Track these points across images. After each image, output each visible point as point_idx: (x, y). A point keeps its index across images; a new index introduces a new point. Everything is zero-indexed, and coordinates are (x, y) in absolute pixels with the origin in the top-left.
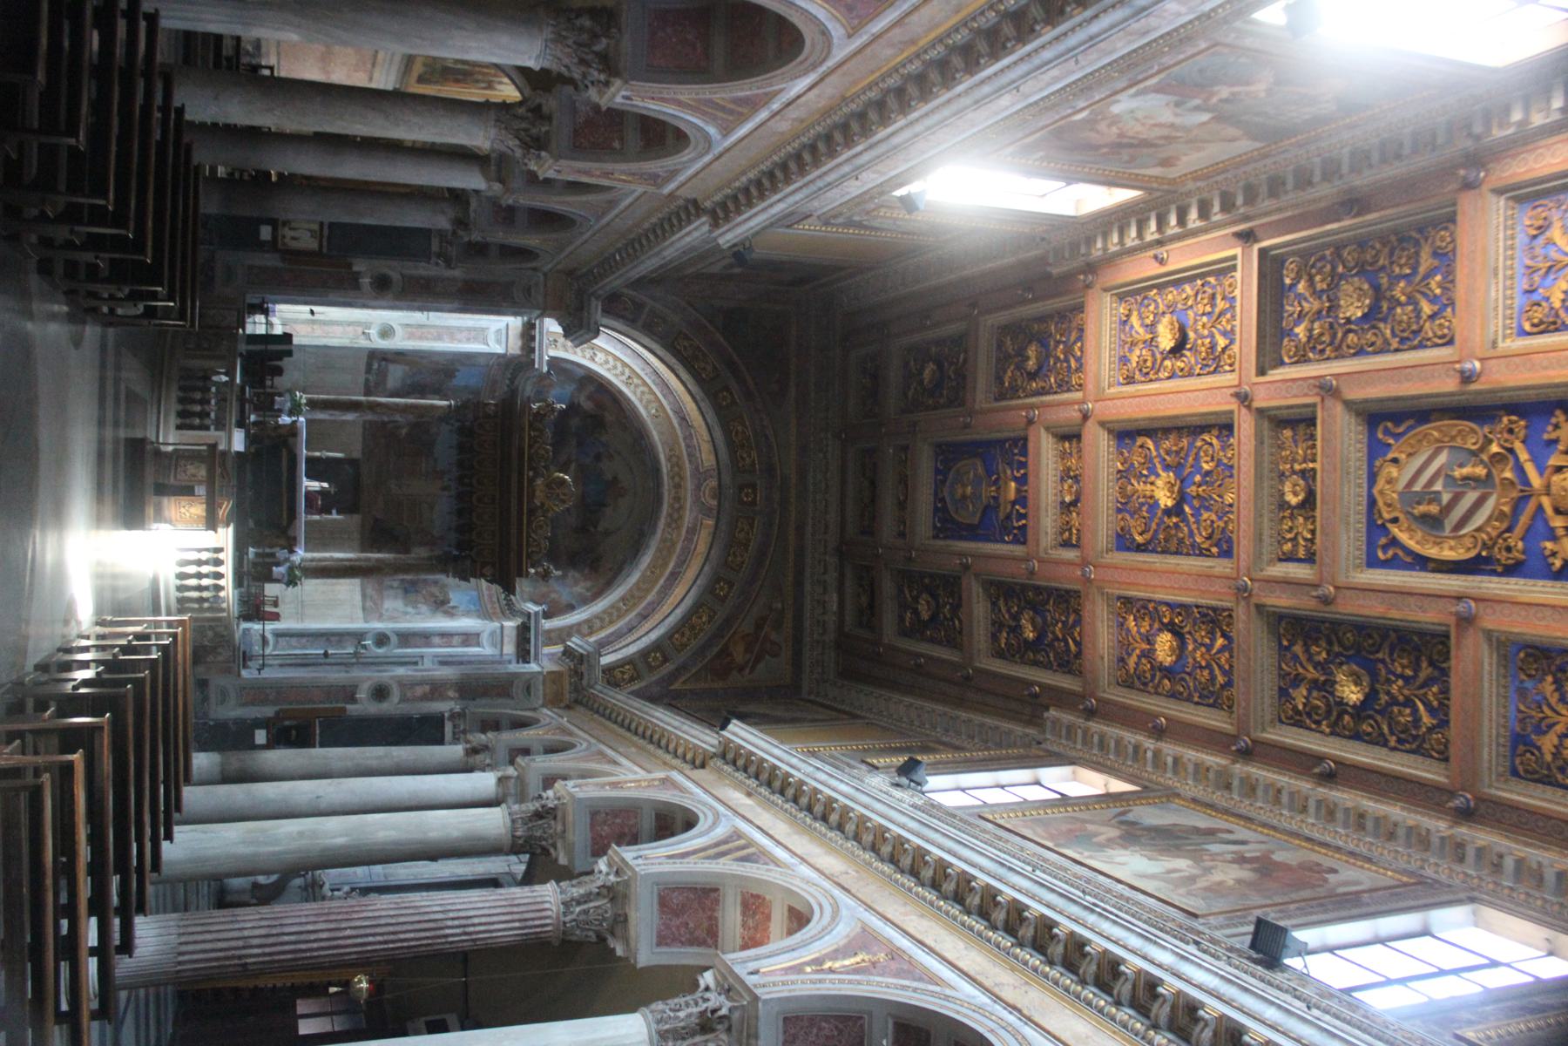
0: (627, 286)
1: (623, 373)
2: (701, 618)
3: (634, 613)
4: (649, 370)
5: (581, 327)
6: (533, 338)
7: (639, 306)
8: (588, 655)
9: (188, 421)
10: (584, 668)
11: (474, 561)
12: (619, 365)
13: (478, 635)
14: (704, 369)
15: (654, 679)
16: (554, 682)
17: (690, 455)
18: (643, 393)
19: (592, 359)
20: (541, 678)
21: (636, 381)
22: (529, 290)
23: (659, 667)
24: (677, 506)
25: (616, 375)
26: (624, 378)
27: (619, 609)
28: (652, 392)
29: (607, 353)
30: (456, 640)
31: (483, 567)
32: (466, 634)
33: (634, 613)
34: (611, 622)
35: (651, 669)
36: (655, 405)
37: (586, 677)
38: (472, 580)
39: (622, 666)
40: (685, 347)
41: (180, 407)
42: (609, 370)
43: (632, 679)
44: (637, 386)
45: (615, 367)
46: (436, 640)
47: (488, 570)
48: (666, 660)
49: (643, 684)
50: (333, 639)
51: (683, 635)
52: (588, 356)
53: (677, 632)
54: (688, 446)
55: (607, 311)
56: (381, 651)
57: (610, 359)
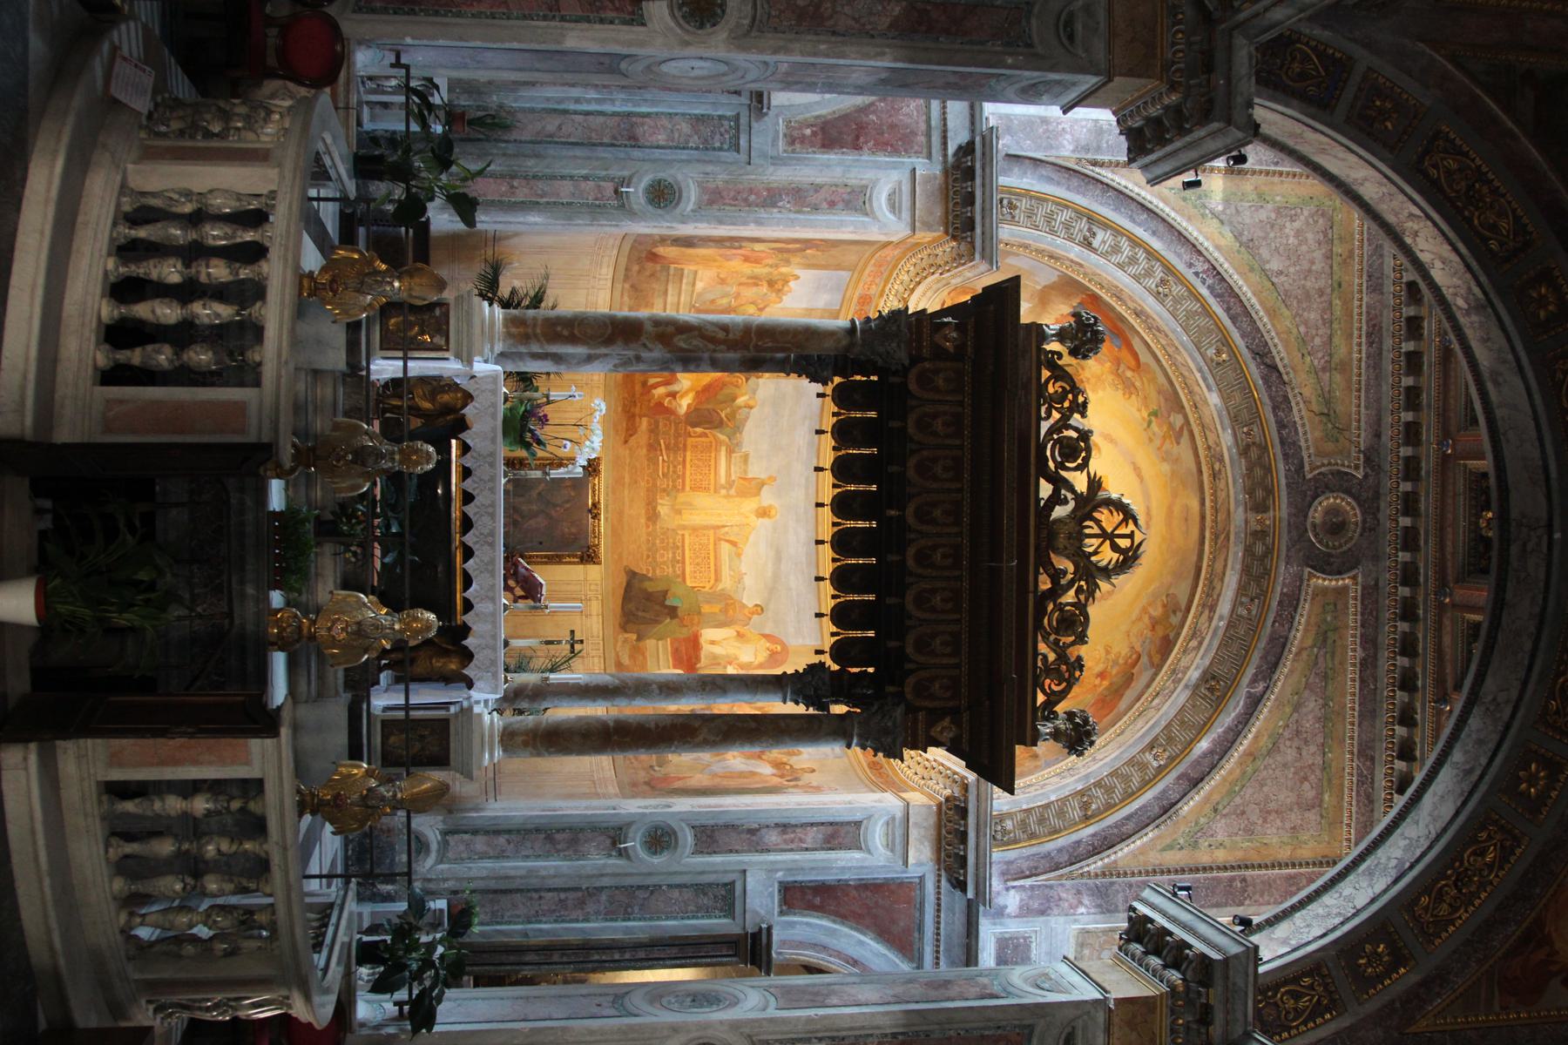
0: (1310, 19)
1: (1149, 273)
2: (1483, 853)
3: (1174, 774)
4: (1201, 266)
5: (1206, 116)
6: (970, 200)
7: (1338, 67)
8: (1227, 961)
9: (135, 357)
10: (1215, 996)
11: (911, 710)
12: (1141, 255)
13: (858, 824)
14: (1494, 228)
15: (1370, 1007)
16: (1131, 1024)
17: (1283, 442)
18: (1190, 315)
19: (1087, 244)
20: (1101, 1017)
21: (1177, 290)
22: (1069, 23)
23: (1379, 978)
24: (1259, 549)
25: (1136, 278)
26: (1151, 283)
27: (1143, 766)
28: (1206, 311)
29: (1118, 231)
30: (812, 836)
31: (930, 724)
32: (831, 824)
33: (1174, 774)
34: (1129, 796)
35: (1364, 983)
36: (1214, 338)
37: (1219, 1016)
38: (907, 753)
39: (1296, 979)
40: (1449, 172)
41: (108, 311)
42: (1120, 266)
43: (1316, 1012)
44: (1177, 301)
45: (1133, 260)
46: (773, 837)
47: (944, 728)
48: (1399, 958)
49: (1345, 1022)
50: (558, 837)
51: (1440, 897)
52: (1080, 237)
53: (1427, 890)
54: (1281, 425)
55: (1275, 83)
56: (657, 860)
57: (1124, 243)
